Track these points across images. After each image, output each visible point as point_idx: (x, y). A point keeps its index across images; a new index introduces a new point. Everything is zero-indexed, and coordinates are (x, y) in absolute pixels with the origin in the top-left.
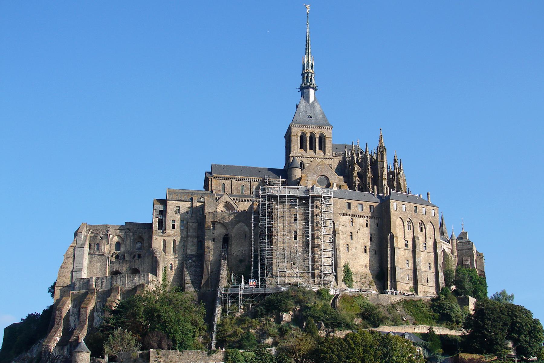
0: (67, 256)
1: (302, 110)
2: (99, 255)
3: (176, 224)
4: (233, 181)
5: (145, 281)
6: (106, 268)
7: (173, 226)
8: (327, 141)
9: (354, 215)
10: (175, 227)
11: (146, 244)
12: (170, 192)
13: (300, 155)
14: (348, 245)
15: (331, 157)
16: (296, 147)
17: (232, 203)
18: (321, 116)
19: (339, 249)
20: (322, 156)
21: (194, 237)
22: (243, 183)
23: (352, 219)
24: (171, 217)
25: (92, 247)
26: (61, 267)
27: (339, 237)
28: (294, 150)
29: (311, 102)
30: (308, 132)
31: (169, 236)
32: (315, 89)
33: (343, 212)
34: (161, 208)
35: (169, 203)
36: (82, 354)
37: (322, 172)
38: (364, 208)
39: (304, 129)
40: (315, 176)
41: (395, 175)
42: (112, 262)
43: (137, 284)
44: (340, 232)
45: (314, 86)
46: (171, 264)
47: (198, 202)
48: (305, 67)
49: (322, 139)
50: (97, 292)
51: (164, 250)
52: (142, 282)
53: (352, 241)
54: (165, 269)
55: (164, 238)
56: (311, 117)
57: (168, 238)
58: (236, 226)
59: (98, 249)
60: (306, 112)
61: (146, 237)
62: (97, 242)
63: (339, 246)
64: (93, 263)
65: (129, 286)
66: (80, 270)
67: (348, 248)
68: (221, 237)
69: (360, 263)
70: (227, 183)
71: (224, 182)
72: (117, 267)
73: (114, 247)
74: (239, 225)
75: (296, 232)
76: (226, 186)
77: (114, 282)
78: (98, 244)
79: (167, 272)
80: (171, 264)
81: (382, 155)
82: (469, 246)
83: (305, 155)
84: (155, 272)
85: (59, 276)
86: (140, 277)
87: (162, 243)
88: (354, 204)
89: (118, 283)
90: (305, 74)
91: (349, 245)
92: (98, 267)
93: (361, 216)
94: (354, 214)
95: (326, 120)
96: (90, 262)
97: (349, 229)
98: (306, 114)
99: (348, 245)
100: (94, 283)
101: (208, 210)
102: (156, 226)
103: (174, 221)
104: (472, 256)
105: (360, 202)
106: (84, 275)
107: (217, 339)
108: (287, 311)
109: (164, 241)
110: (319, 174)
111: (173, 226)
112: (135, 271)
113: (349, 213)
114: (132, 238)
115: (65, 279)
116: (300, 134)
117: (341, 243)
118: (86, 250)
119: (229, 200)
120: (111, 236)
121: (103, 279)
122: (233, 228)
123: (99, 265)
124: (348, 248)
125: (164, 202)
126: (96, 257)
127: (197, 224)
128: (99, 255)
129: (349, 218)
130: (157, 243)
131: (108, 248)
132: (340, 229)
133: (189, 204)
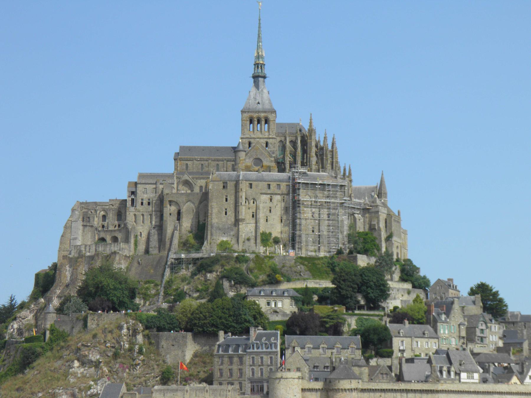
0: (66, 227)
1: (252, 97)
2: (89, 226)
3: (144, 202)
4: (195, 161)
5: (118, 248)
6: (95, 236)
7: (142, 204)
8: (271, 123)
9: (272, 194)
10: (144, 204)
11: (123, 217)
12: (141, 176)
13: (248, 136)
14: (267, 217)
15: (274, 136)
16: (246, 130)
17: (190, 181)
18: (267, 102)
19: (259, 221)
20: (266, 136)
21: (157, 211)
22: (202, 162)
23: (271, 197)
24: (140, 196)
25: (84, 220)
26: (62, 236)
27: (259, 212)
28: (244, 132)
29: (260, 90)
30: (255, 115)
31: (139, 211)
32: (264, 77)
33: (264, 192)
34: (134, 190)
35: (139, 186)
36: (50, 314)
37: (257, 156)
38: (282, 187)
39: (252, 114)
40: (252, 159)
41: (324, 150)
42: (99, 231)
43: (113, 251)
44: (261, 208)
45: (263, 75)
46: (141, 233)
47: (160, 184)
48: (258, 57)
49: (267, 121)
50: (85, 256)
51: (135, 222)
52: (116, 249)
53: (270, 214)
54: (136, 237)
55: (135, 213)
56: (259, 103)
57: (138, 213)
58: (187, 204)
59: (89, 222)
60: (255, 99)
61: (123, 212)
62: (88, 216)
63: (259, 219)
64: (85, 232)
65: (108, 252)
66: (75, 239)
67: (267, 220)
68: (176, 212)
69: (277, 230)
70: (189, 163)
71: (187, 162)
72: (102, 235)
73: (101, 219)
74: (189, 203)
75: (226, 209)
76: (189, 165)
77: (97, 249)
78: (89, 218)
79: (138, 239)
80: (141, 233)
81: (311, 136)
82: (377, 210)
83: (253, 136)
84: (127, 240)
85: (61, 243)
86: (114, 246)
87: (134, 217)
88: (273, 185)
89: (100, 249)
90: (257, 65)
91: (269, 218)
92: (89, 235)
93: (278, 194)
94: (272, 193)
95: (271, 106)
96: (84, 231)
97: (269, 204)
98: (255, 100)
99: (267, 217)
100: (83, 249)
101: (166, 191)
102: (129, 203)
103: (142, 199)
104: (378, 218)
105: (278, 183)
106: (79, 243)
107: (164, 293)
108: (211, 272)
109: (135, 215)
110: (255, 157)
111: (142, 204)
112: (115, 239)
113: (269, 192)
114: (114, 212)
115: (65, 245)
116: (249, 120)
117: (261, 215)
118: (80, 223)
119: (188, 178)
120: (98, 212)
121: (90, 246)
122: (184, 205)
123: (90, 233)
124: (267, 220)
125: (136, 184)
126: (88, 228)
127: (160, 201)
128: (89, 226)
129: (269, 196)
130: (130, 218)
131: (97, 222)
132: (261, 206)
133: (154, 186)
